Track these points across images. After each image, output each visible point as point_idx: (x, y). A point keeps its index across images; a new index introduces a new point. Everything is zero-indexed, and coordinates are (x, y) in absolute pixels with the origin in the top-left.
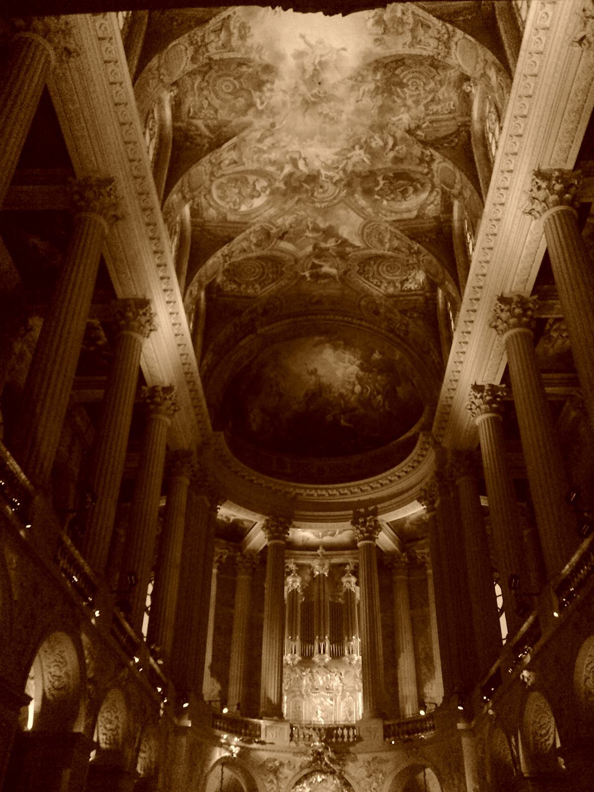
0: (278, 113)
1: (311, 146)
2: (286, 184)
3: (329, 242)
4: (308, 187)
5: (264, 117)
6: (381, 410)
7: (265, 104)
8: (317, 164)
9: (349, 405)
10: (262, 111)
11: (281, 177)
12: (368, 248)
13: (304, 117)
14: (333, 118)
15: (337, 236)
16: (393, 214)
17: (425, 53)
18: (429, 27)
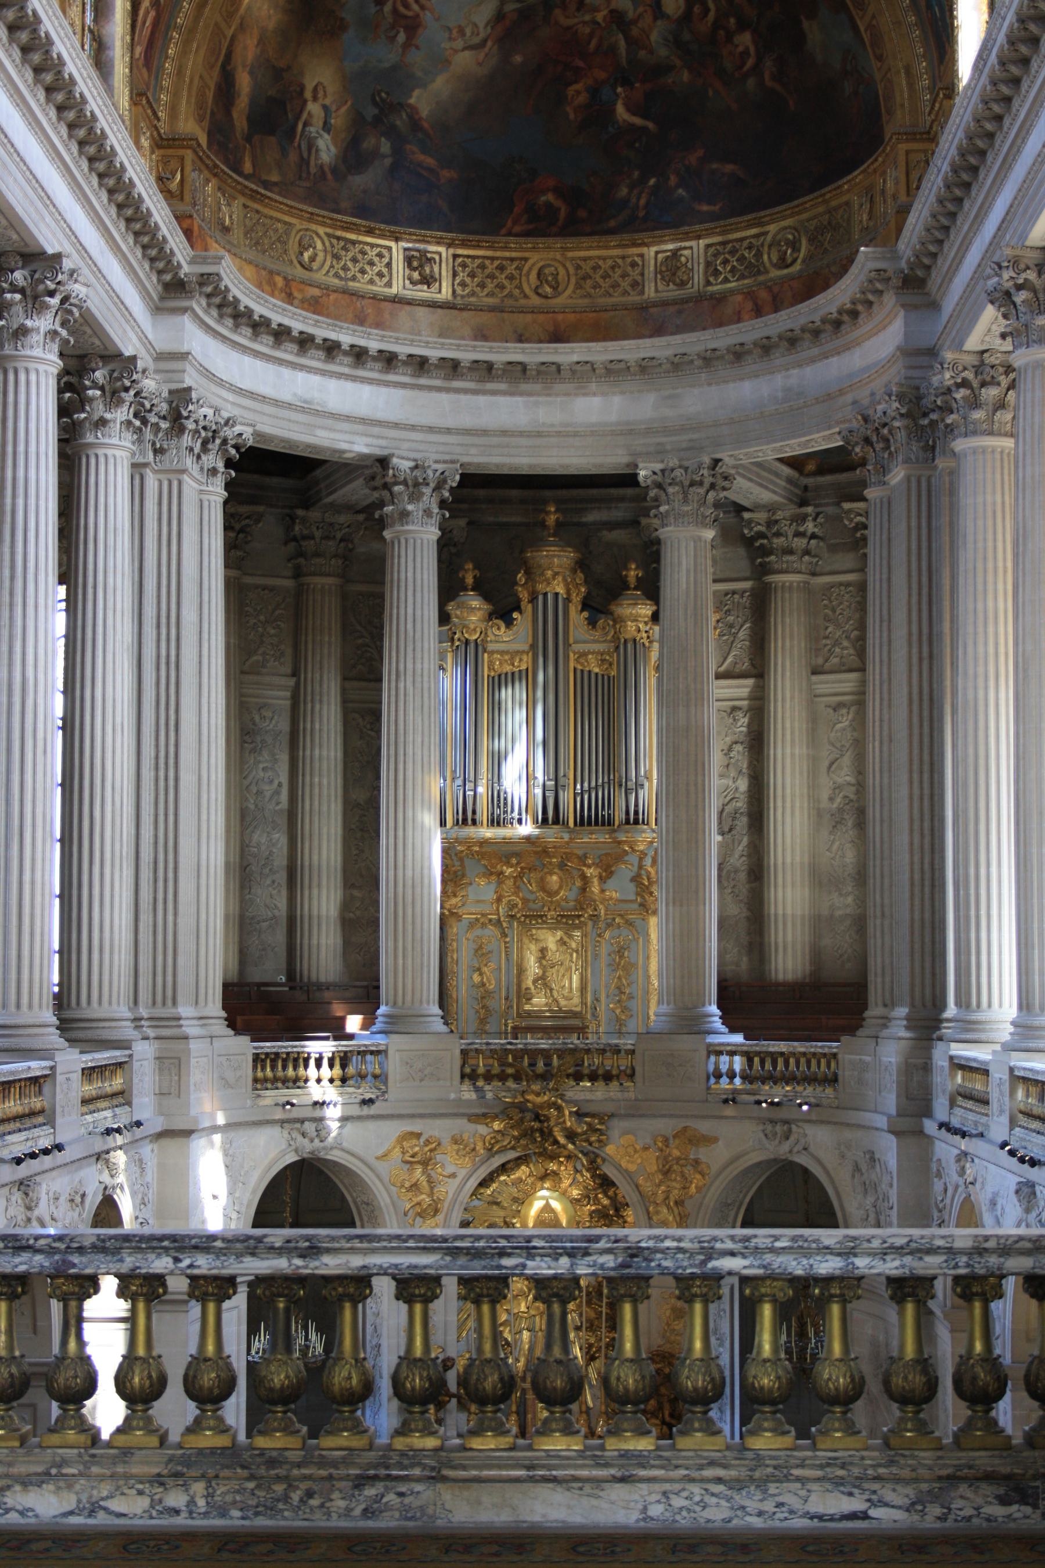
6: (751, 83)
9: (642, 54)
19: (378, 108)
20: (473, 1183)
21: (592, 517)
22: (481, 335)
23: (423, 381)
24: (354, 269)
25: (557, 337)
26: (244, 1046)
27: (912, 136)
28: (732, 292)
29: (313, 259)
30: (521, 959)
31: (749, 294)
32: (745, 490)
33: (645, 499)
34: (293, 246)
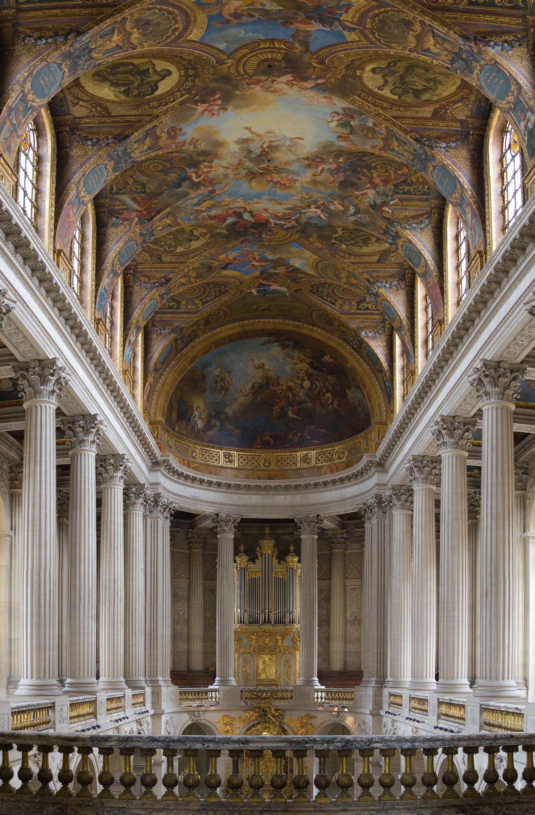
0: (219, 183)
1: (257, 203)
2: (227, 230)
3: (279, 269)
4: (255, 231)
5: (203, 188)
7: (202, 177)
8: (265, 215)
10: (199, 182)
11: (223, 226)
12: (322, 277)
13: (250, 183)
14: (285, 185)
15: (288, 266)
16: (352, 257)
17: (397, 159)
18: (406, 144)
19: (216, 413)
20: (244, 730)
21: (280, 531)
22: (247, 477)
23: (229, 491)
24: (208, 458)
25: (270, 478)
26: (175, 689)
27: (380, 423)
28: (324, 466)
29: (196, 455)
30: (258, 663)
31: (329, 466)
32: (327, 524)
33: (296, 526)
34: (190, 452)
